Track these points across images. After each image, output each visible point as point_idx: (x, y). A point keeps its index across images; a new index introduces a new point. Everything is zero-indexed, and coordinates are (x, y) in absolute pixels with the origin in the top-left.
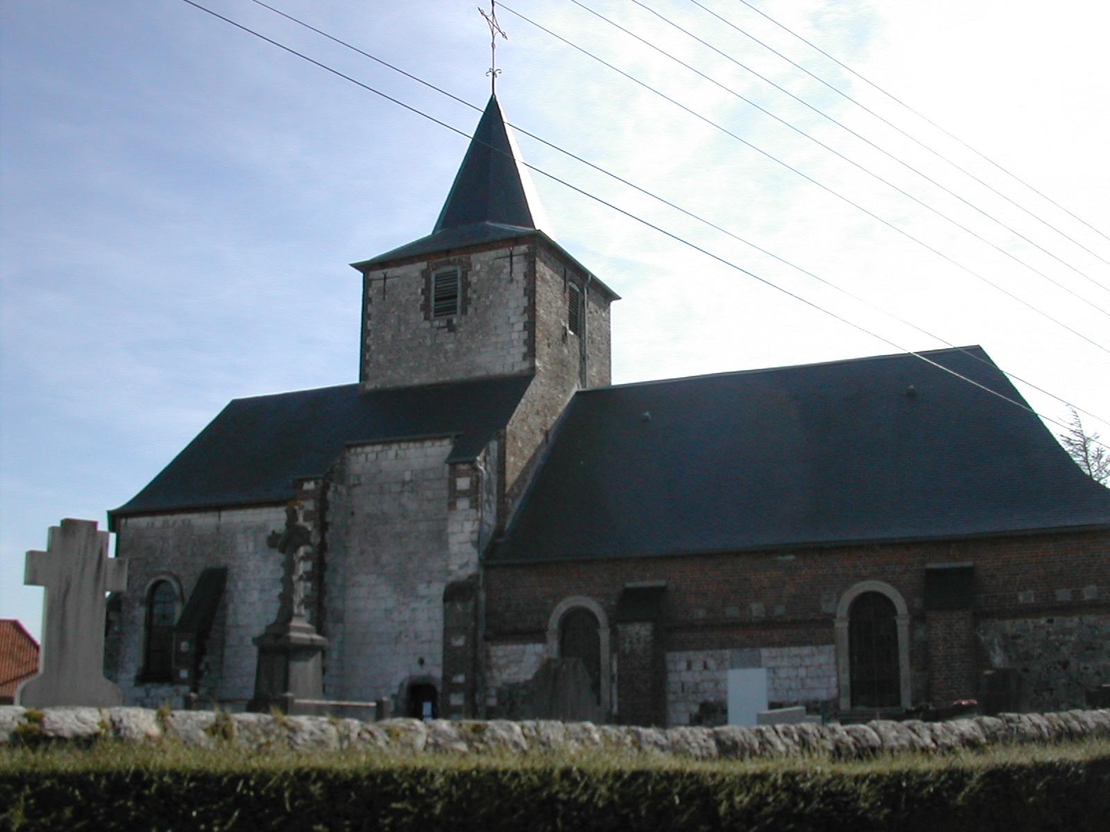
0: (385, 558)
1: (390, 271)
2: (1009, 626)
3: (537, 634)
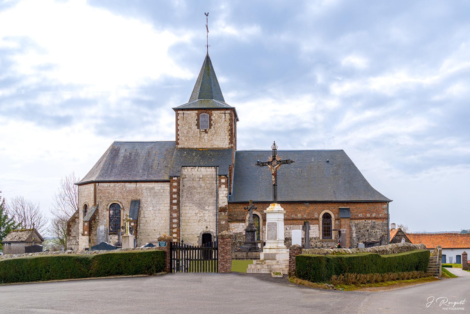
0: (195, 199)
1: (186, 112)
2: (356, 222)
3: (243, 221)
